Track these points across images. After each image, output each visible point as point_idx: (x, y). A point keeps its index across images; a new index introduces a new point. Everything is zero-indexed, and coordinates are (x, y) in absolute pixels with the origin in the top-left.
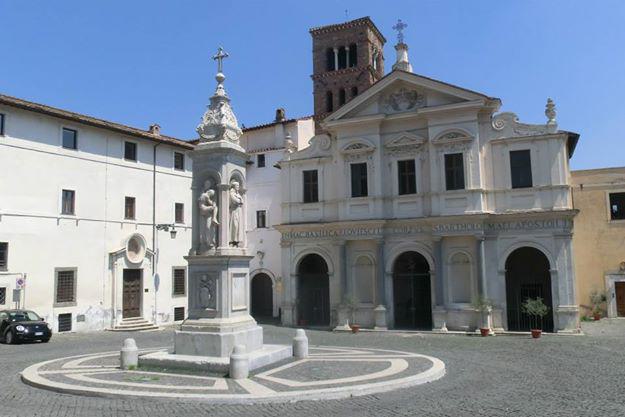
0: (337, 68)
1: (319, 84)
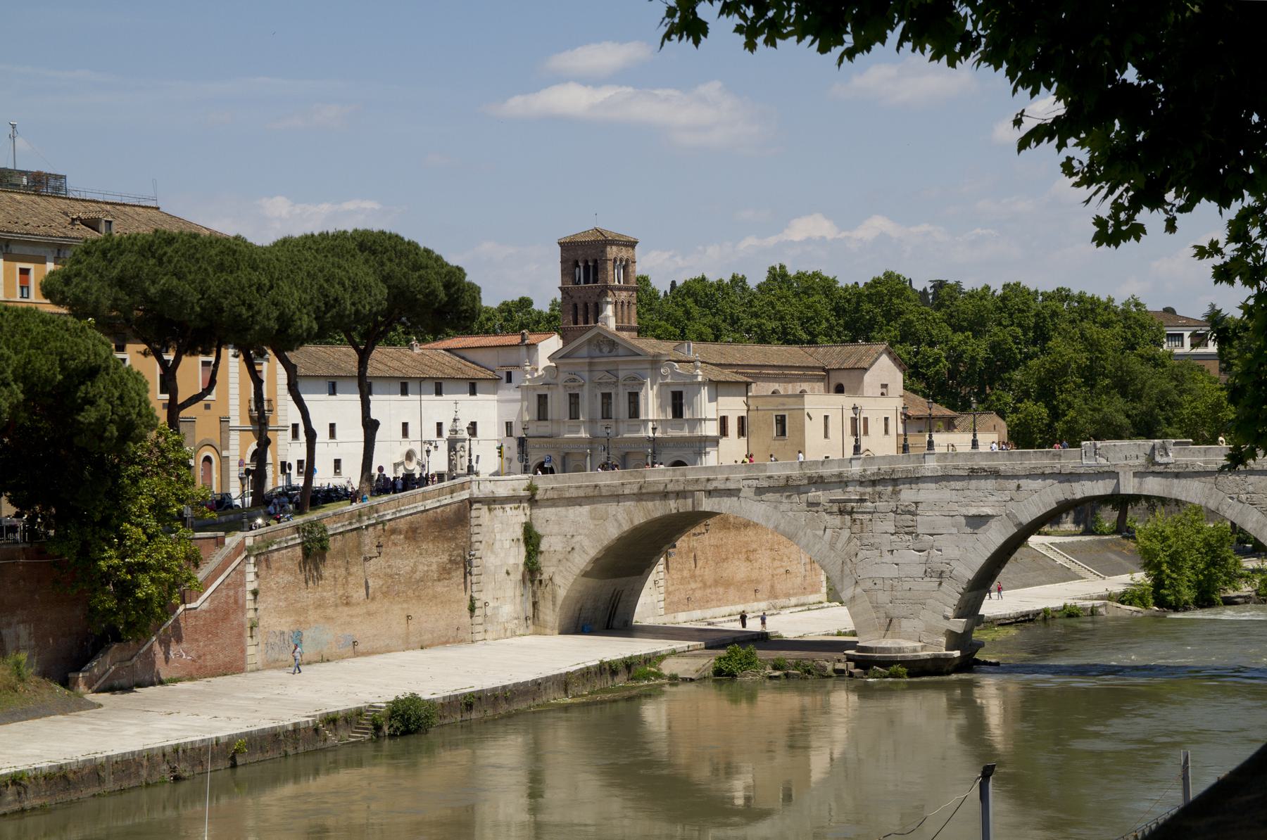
1: (566, 295)
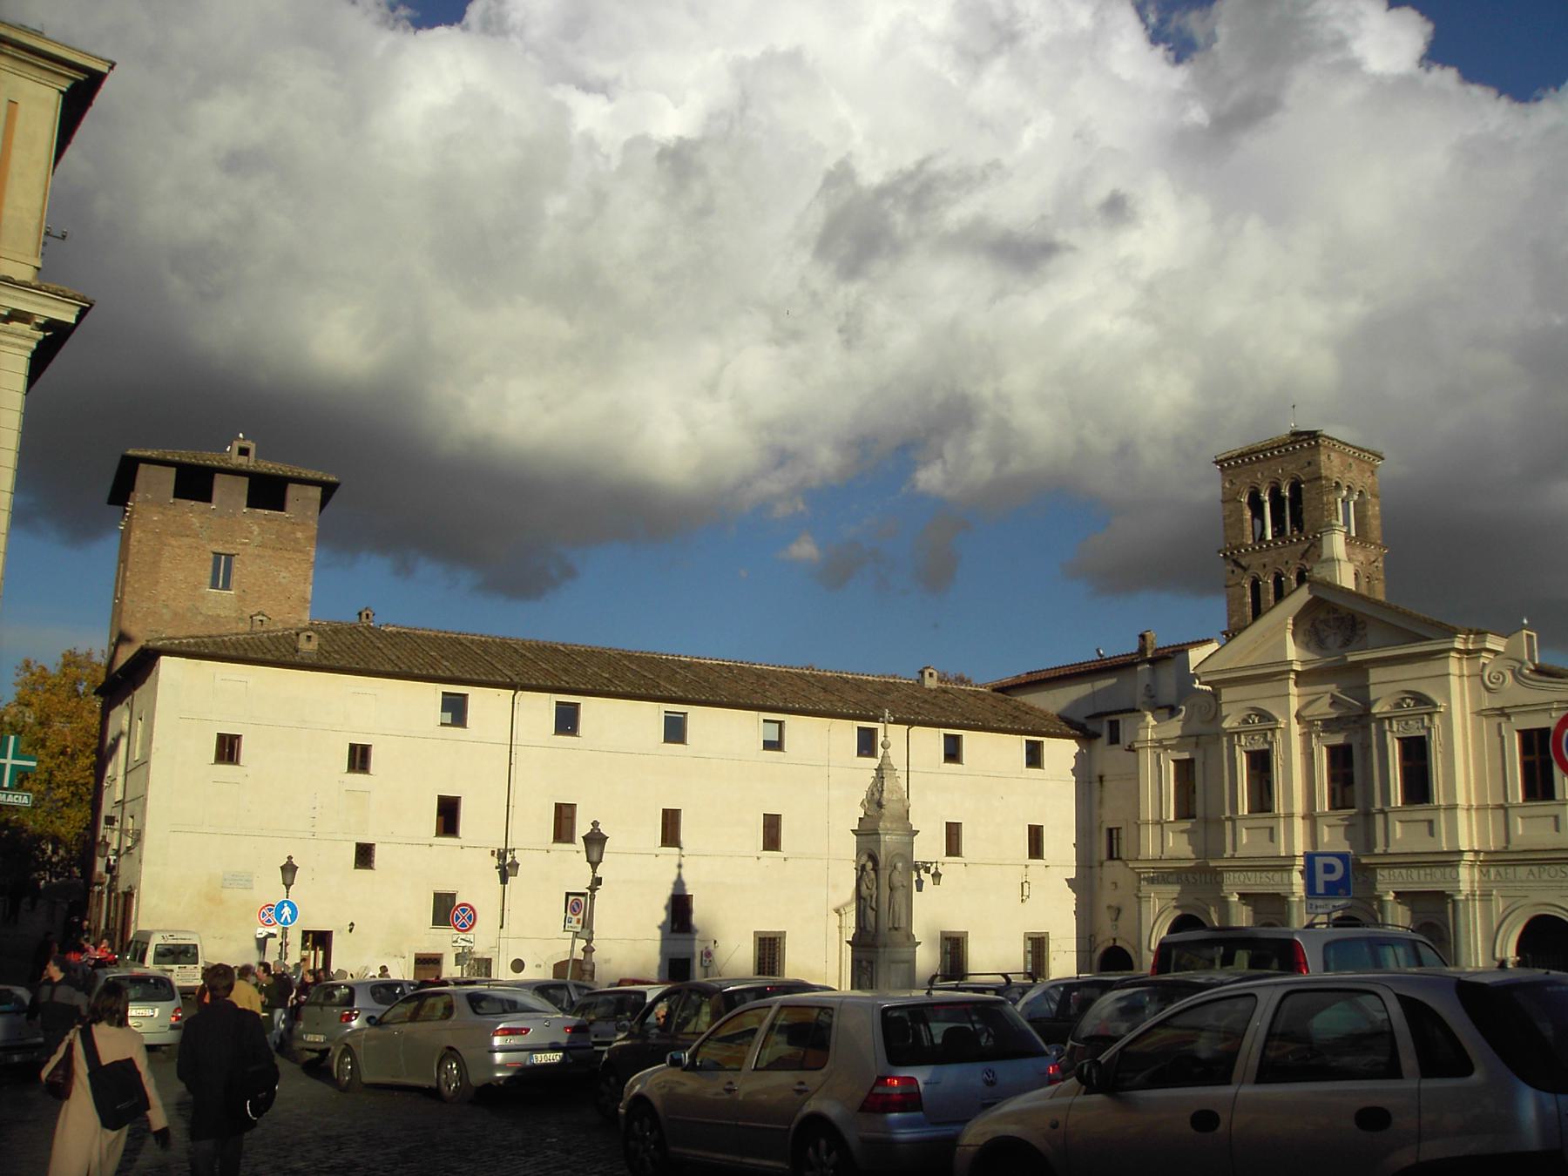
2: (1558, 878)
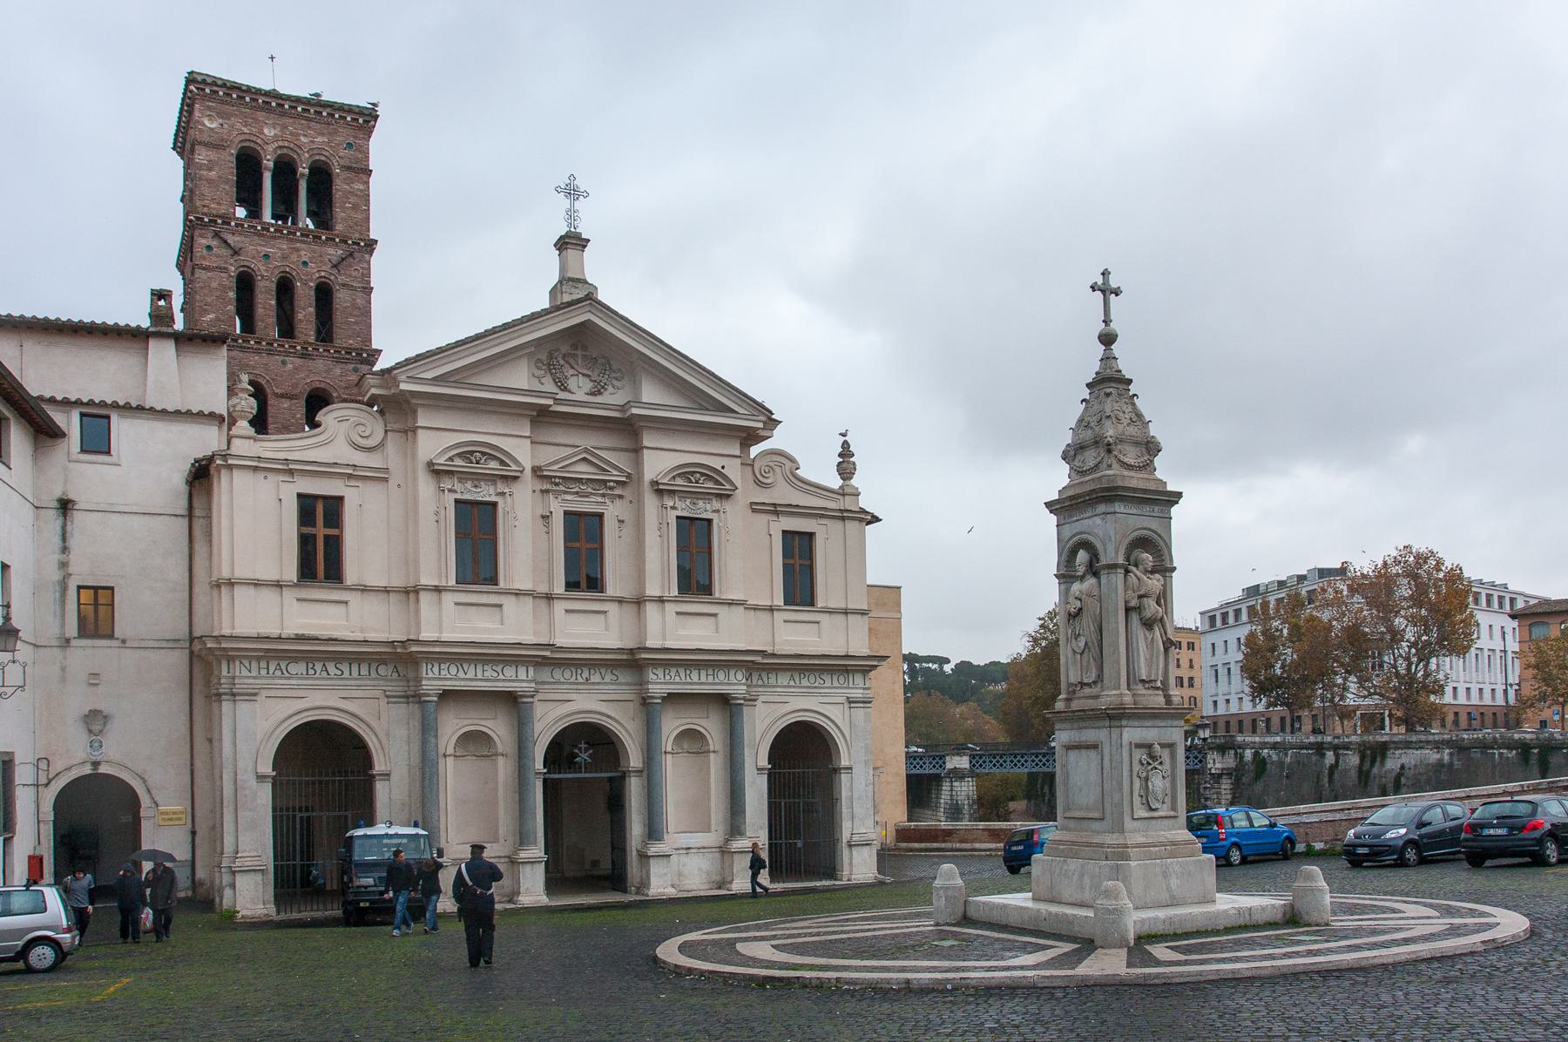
0: (267, 216)
1: (214, 243)
2: (816, 684)
